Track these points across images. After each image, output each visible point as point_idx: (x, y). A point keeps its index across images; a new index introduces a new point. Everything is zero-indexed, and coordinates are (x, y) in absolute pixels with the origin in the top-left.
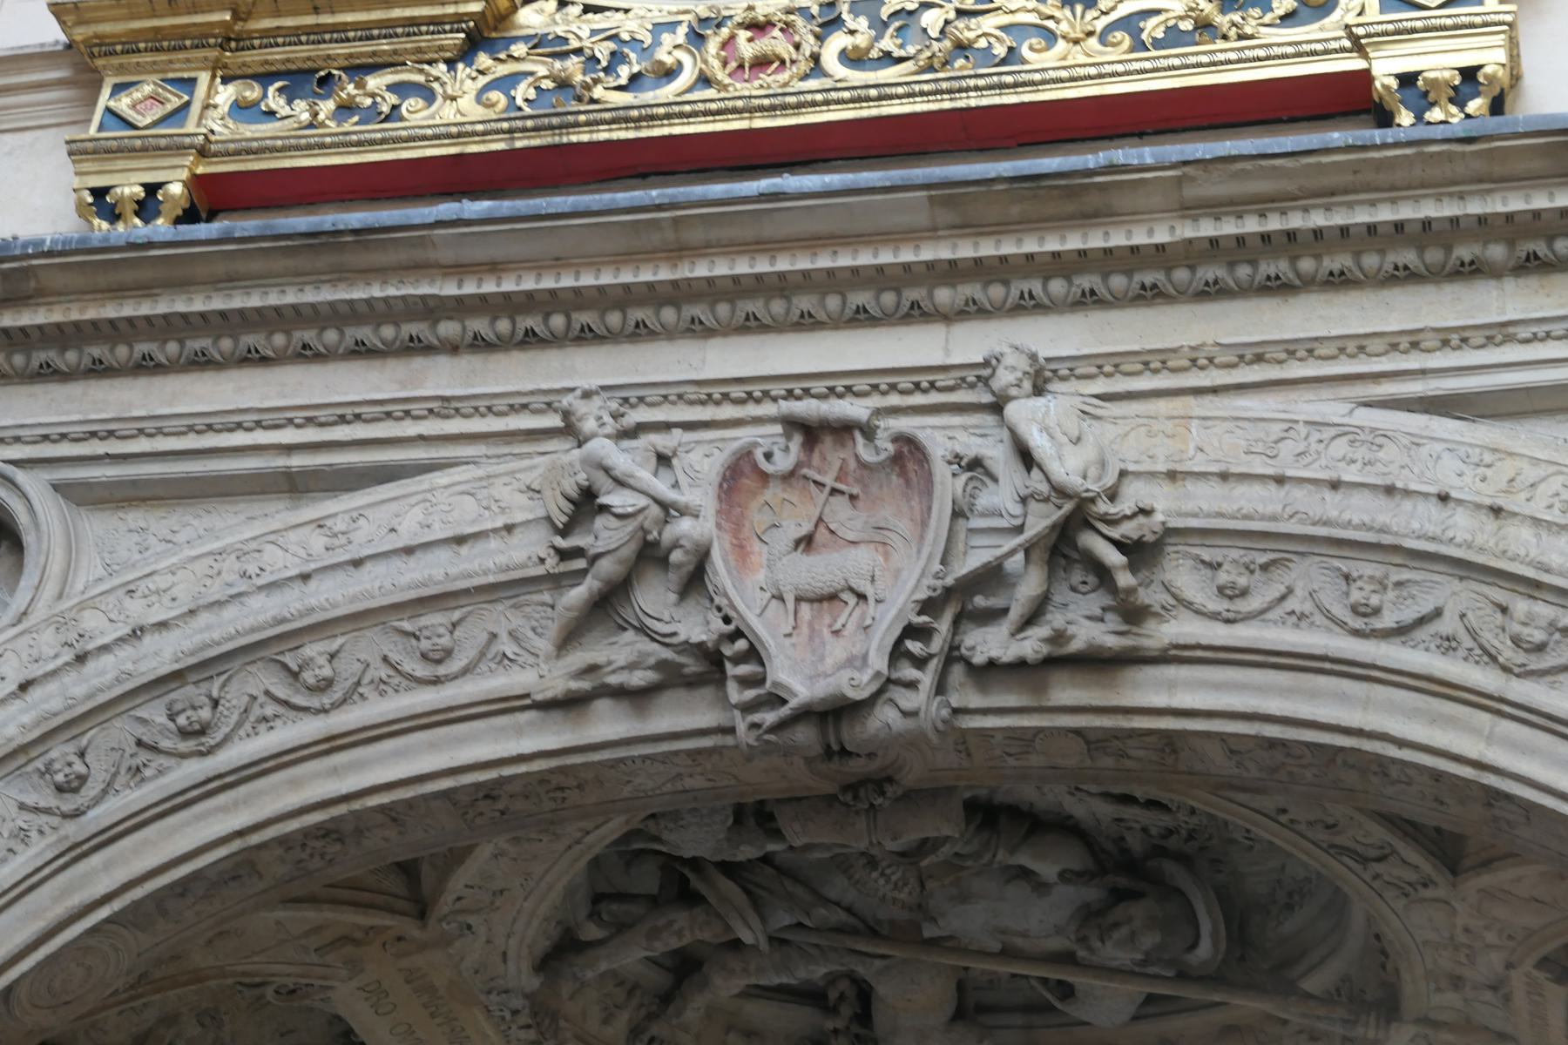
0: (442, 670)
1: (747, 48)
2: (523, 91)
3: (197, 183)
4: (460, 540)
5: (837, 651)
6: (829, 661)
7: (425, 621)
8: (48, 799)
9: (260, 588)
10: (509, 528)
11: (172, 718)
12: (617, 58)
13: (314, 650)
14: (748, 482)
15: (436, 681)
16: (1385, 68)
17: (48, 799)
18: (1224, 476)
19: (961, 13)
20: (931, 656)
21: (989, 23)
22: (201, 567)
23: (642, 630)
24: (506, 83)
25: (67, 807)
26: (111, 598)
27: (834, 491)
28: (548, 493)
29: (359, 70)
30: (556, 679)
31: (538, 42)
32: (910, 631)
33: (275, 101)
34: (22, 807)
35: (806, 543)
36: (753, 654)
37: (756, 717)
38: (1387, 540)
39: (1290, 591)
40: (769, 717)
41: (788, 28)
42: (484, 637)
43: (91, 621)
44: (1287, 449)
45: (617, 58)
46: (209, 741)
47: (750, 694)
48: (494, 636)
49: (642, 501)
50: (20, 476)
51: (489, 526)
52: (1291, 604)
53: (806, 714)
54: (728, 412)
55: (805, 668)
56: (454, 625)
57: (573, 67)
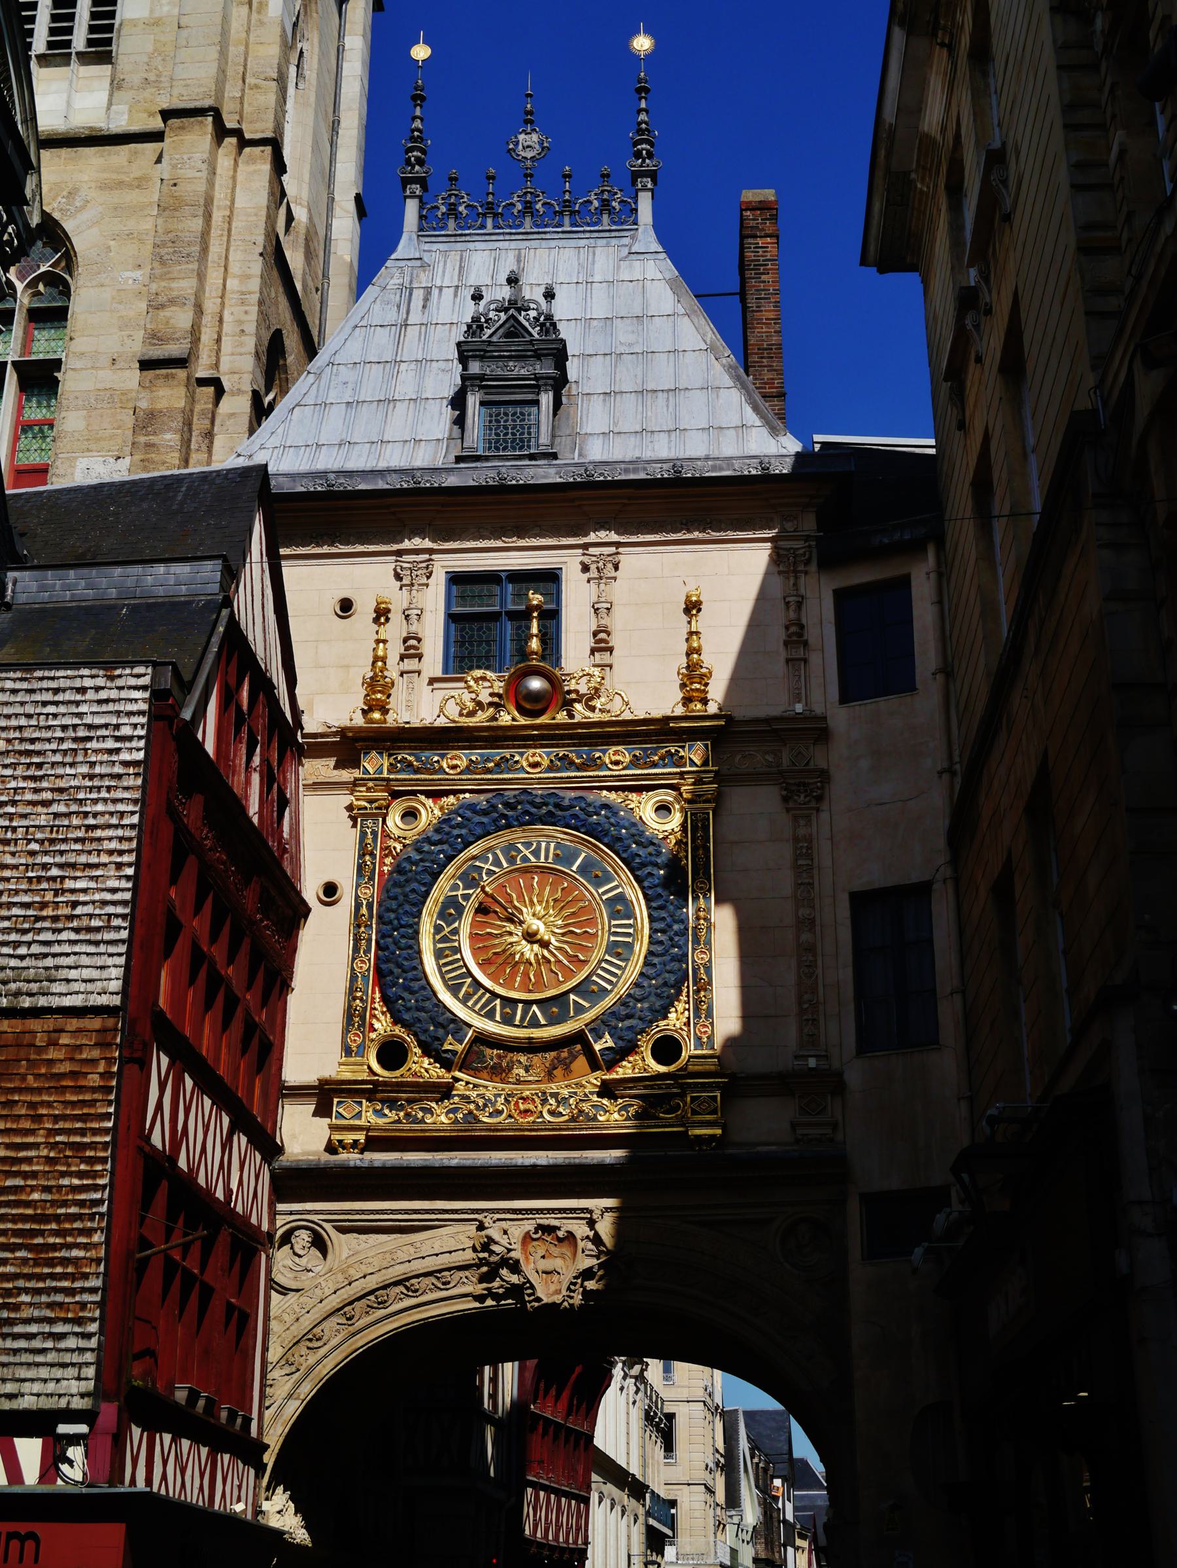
1: (522, 1107)
3: (368, 1138)
5: (553, 1288)
12: (485, 1105)
13: (413, 1281)
24: (454, 1111)
29: (410, 1101)
30: (479, 1289)
31: (462, 1097)
32: (572, 1283)
33: (386, 1111)
35: (543, 1257)
36: (532, 1287)
40: (536, 1304)
43: (352, 1271)
45: (485, 1105)
50: (325, 1224)
53: (546, 1304)
54: (520, 1216)
55: (547, 1292)
57: (472, 1106)
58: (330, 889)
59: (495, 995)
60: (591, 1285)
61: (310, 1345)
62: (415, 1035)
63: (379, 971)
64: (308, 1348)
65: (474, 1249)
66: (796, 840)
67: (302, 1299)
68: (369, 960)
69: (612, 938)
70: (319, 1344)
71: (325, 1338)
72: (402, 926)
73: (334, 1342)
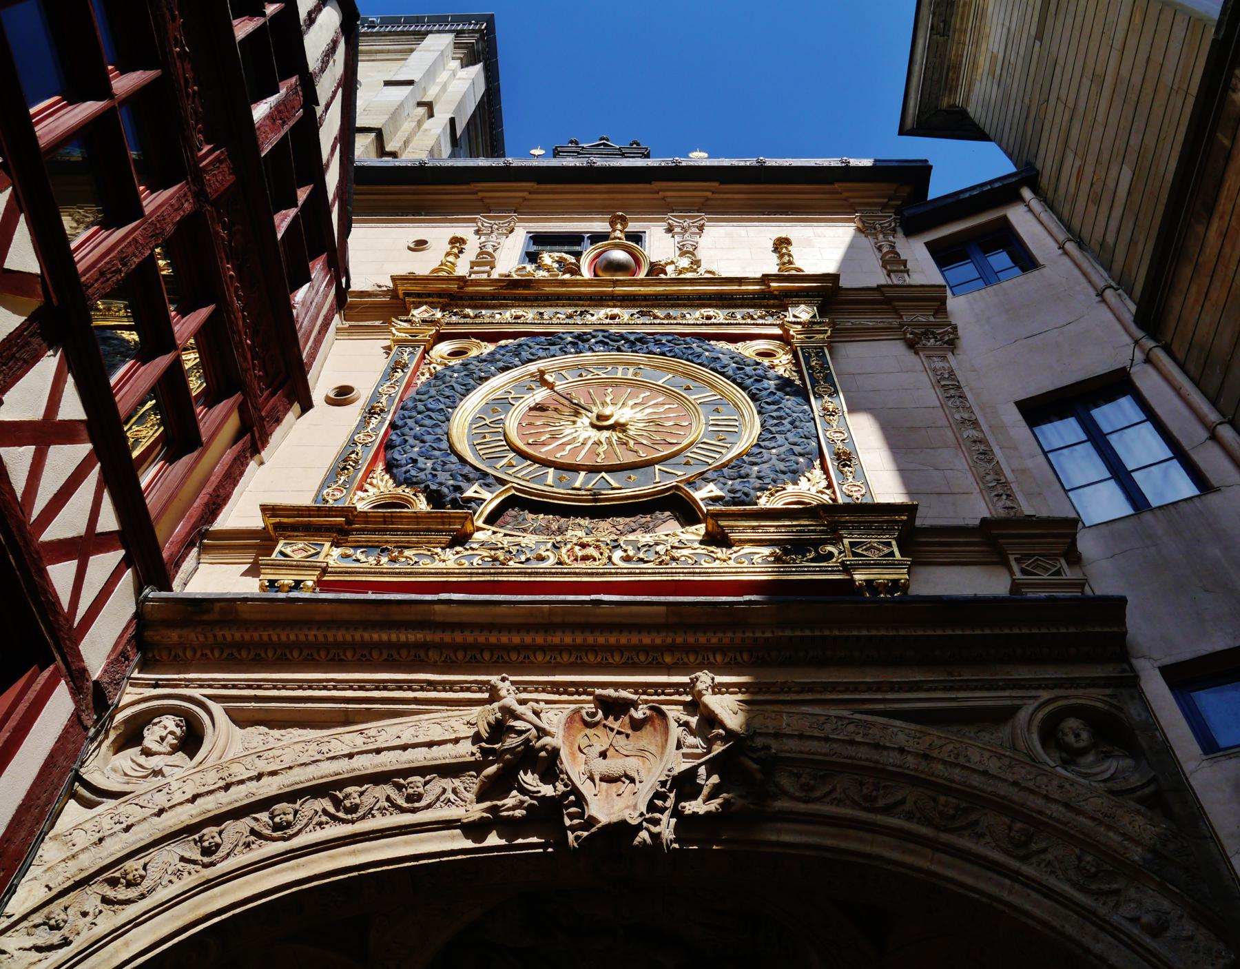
0: (416, 805)
1: (579, 552)
2: (476, 561)
4: (430, 745)
6: (616, 808)
7: (410, 779)
8: (196, 855)
9: (328, 759)
10: (456, 741)
11: (272, 818)
14: (579, 725)
15: (414, 811)
16: (859, 577)
17: (196, 855)
18: (801, 737)
19: (673, 547)
20: (666, 809)
21: (686, 552)
22: (298, 747)
23: (523, 791)
25: (206, 860)
26: (249, 759)
27: (619, 733)
28: (480, 723)
30: (476, 811)
31: (483, 544)
32: (657, 795)
34: (182, 859)
35: (603, 755)
37: (579, 833)
38: (879, 766)
39: (834, 789)
41: (597, 547)
42: (439, 790)
44: (828, 727)
46: (290, 832)
47: (576, 821)
48: (444, 790)
49: (529, 726)
50: (209, 703)
51: (447, 737)
52: (835, 795)
54: (565, 697)
55: (606, 807)
56: (426, 783)
58: (342, 396)
59: (546, 463)
60: (696, 806)
61: (111, 893)
62: (426, 490)
63: (388, 445)
64: (105, 900)
65: (477, 738)
66: (934, 370)
67: (122, 808)
68: (377, 435)
69: (711, 428)
70: (132, 893)
71: (146, 884)
72: (428, 410)
73: (162, 895)
